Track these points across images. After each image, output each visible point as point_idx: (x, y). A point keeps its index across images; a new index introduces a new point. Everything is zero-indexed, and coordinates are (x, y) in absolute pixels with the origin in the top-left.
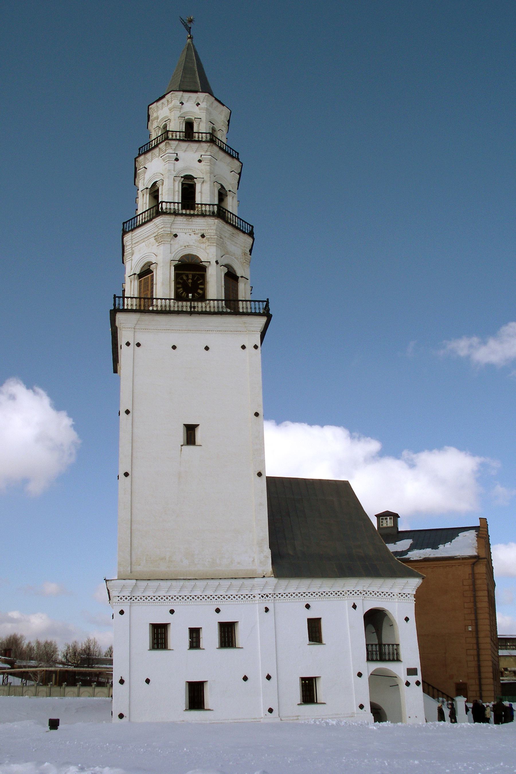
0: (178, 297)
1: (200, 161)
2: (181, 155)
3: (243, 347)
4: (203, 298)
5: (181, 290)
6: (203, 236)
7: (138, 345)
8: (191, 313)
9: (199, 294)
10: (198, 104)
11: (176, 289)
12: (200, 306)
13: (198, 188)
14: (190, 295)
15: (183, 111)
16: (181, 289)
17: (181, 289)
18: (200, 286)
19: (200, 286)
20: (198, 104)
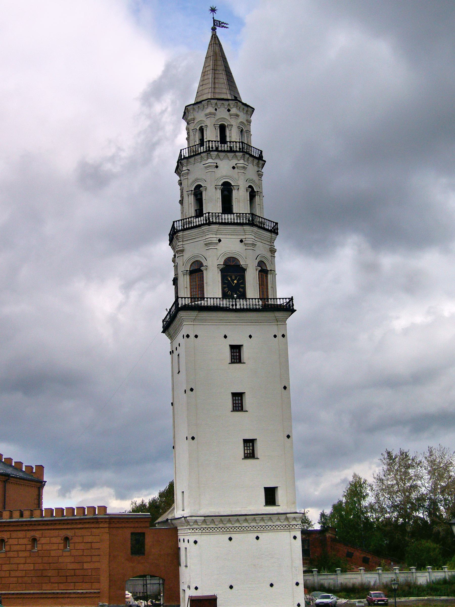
0: (225, 296)
1: (234, 168)
2: (220, 163)
3: (275, 336)
4: (243, 296)
5: (226, 289)
6: (241, 241)
7: (196, 336)
8: (236, 310)
9: (240, 292)
10: (229, 110)
11: (223, 289)
12: (241, 304)
13: (234, 193)
14: (235, 296)
15: (217, 117)
16: (227, 289)
17: (227, 289)
18: (241, 286)
19: (241, 286)
20: (229, 110)
